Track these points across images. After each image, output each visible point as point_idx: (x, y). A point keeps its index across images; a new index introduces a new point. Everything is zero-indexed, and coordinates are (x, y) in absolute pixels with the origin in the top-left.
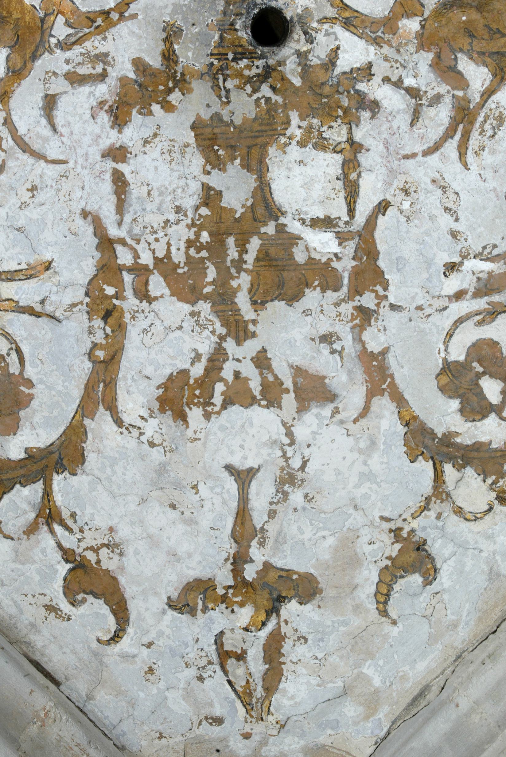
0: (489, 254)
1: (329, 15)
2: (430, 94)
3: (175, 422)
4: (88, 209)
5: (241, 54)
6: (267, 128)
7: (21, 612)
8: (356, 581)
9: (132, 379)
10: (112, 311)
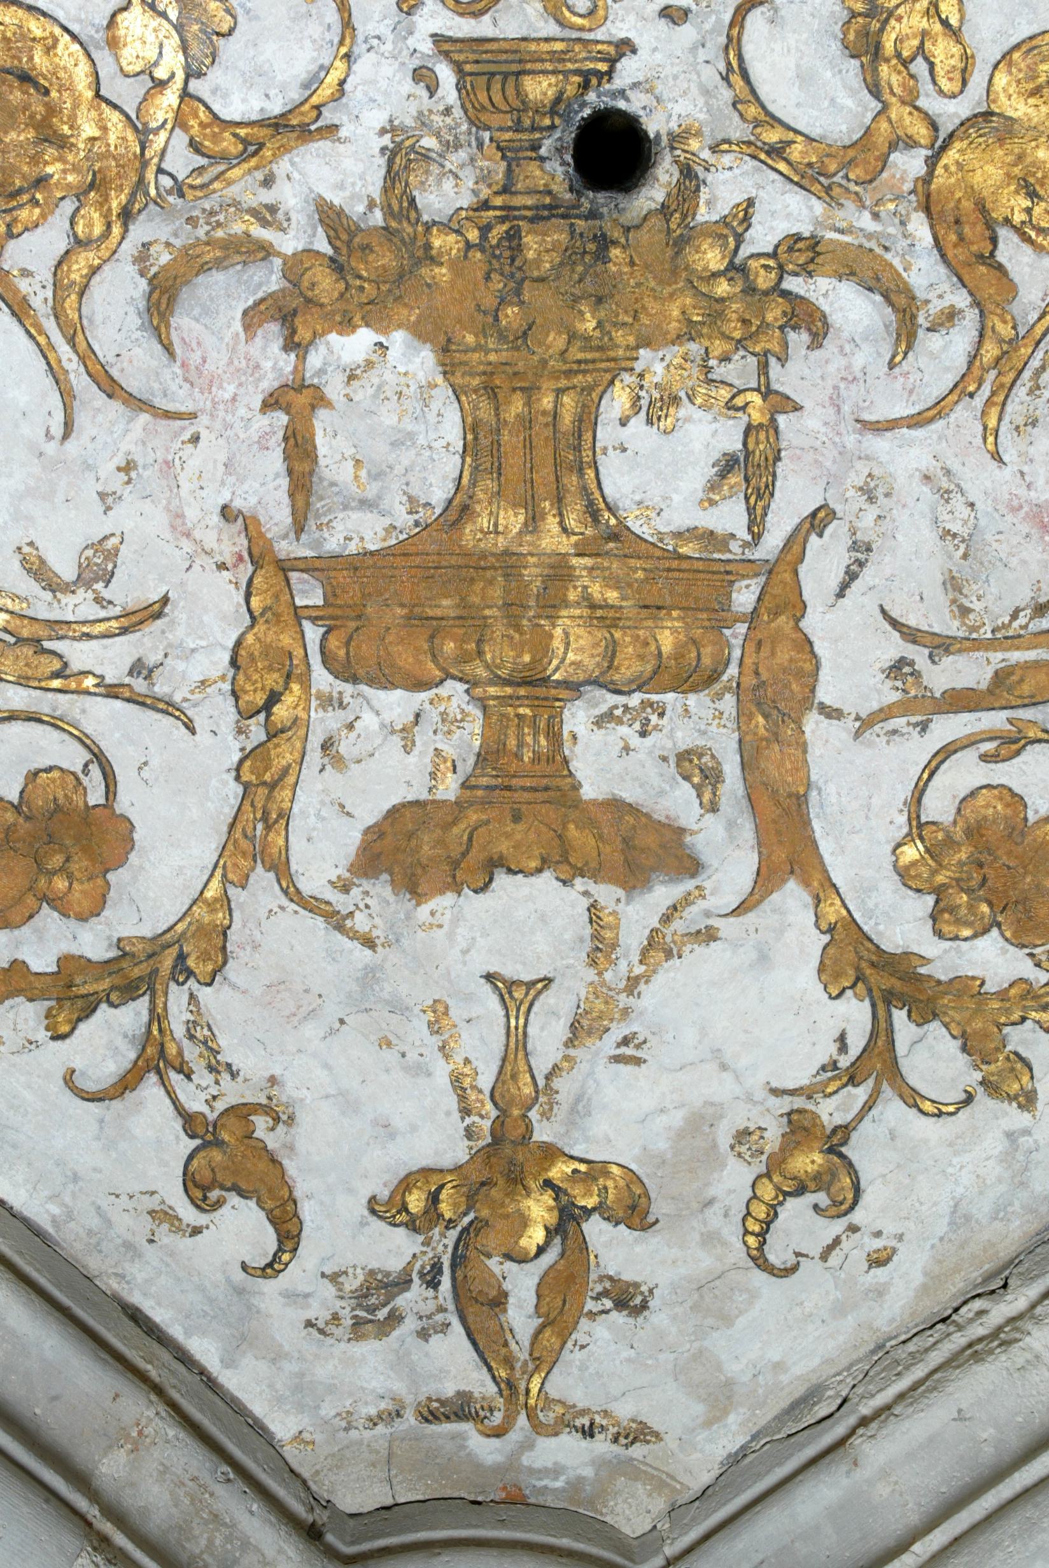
0: (1021, 627)
1: (735, 135)
2: (936, 306)
3: (396, 895)
4: (237, 504)
5: (550, 207)
6: (597, 355)
7: (109, 1223)
8: (711, 1192)
9: (318, 815)
10: (281, 694)
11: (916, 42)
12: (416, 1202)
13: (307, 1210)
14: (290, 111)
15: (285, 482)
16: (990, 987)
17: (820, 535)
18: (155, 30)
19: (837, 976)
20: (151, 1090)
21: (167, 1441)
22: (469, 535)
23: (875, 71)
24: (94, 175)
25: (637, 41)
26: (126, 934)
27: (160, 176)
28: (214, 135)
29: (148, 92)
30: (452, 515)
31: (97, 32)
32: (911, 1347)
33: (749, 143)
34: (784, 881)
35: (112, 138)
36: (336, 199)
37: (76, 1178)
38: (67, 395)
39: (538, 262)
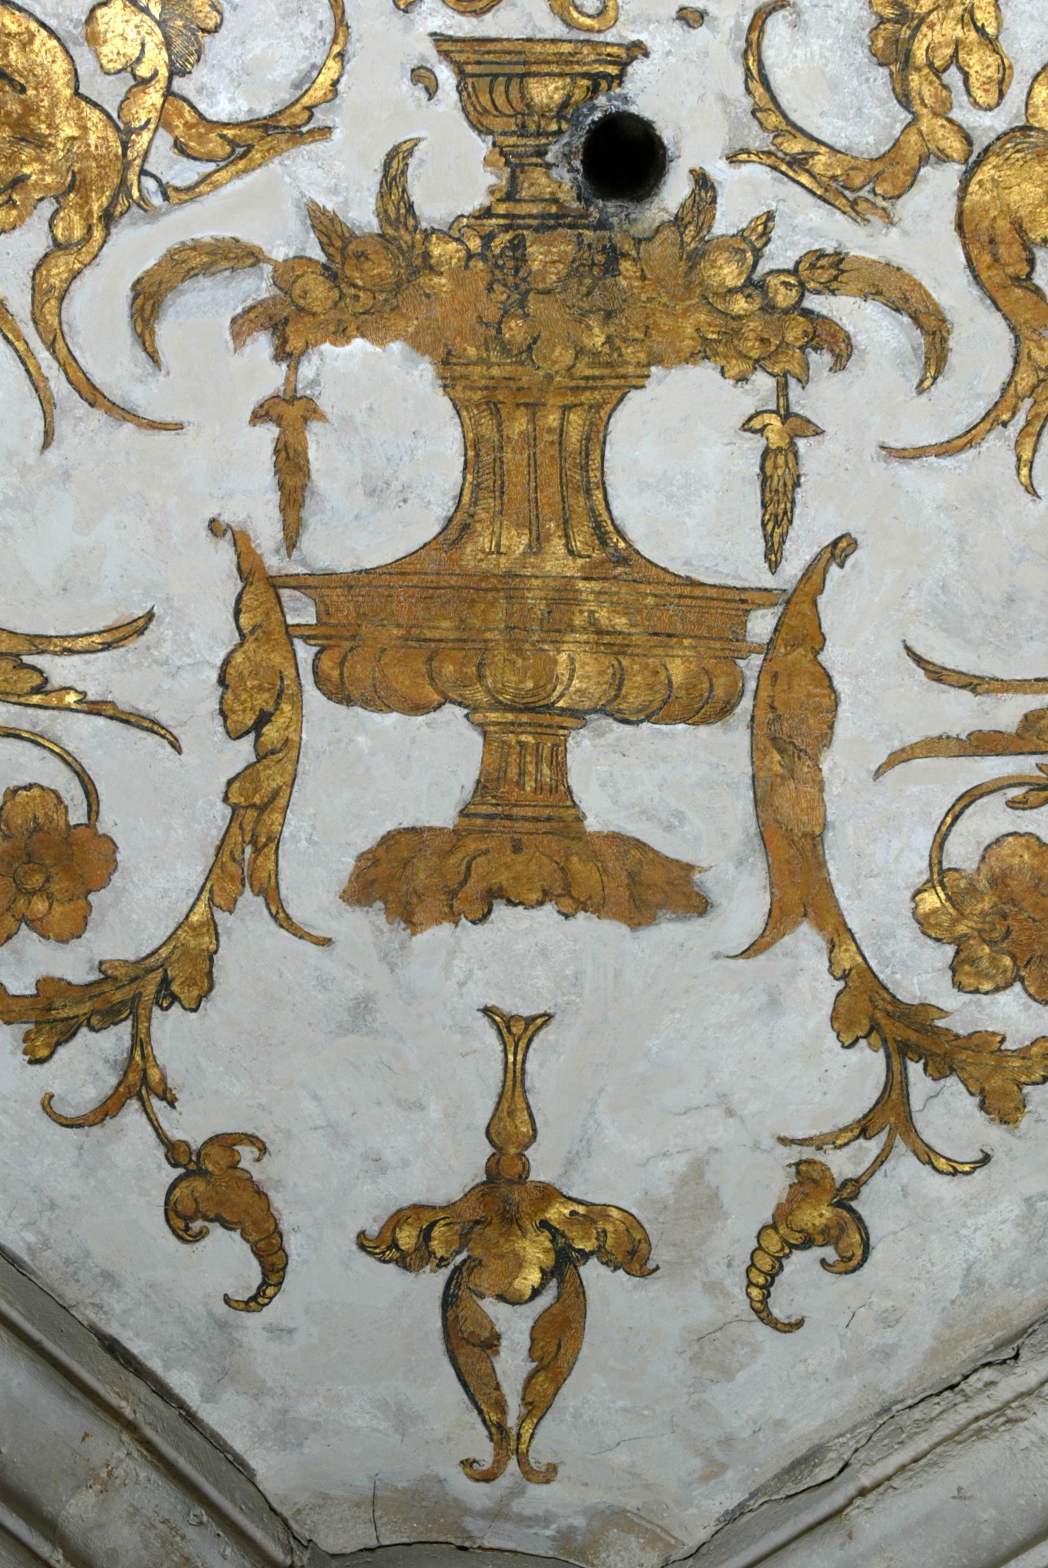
1: (755, 145)
3: (391, 924)
4: (226, 518)
5: (556, 217)
6: (606, 372)
9: (310, 840)
10: (272, 714)
11: (949, 51)
12: (407, 1238)
13: (293, 1244)
14: (280, 112)
15: (275, 497)
16: (1009, 1045)
17: (842, 566)
18: (137, 27)
19: (850, 1025)
20: (132, 1114)
21: (137, 1483)
22: (469, 555)
23: (905, 81)
24: (74, 174)
25: (649, 44)
26: (108, 957)
27: (144, 179)
28: (200, 136)
29: (129, 91)
30: (453, 534)
31: (75, 27)
32: (917, 1414)
33: (769, 153)
34: (797, 924)
35: (93, 139)
36: (329, 204)
37: (53, 1206)
38: (47, 403)
39: (543, 273)
